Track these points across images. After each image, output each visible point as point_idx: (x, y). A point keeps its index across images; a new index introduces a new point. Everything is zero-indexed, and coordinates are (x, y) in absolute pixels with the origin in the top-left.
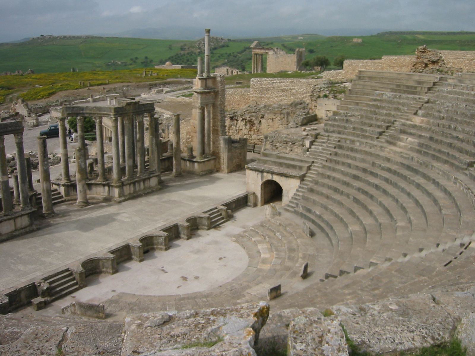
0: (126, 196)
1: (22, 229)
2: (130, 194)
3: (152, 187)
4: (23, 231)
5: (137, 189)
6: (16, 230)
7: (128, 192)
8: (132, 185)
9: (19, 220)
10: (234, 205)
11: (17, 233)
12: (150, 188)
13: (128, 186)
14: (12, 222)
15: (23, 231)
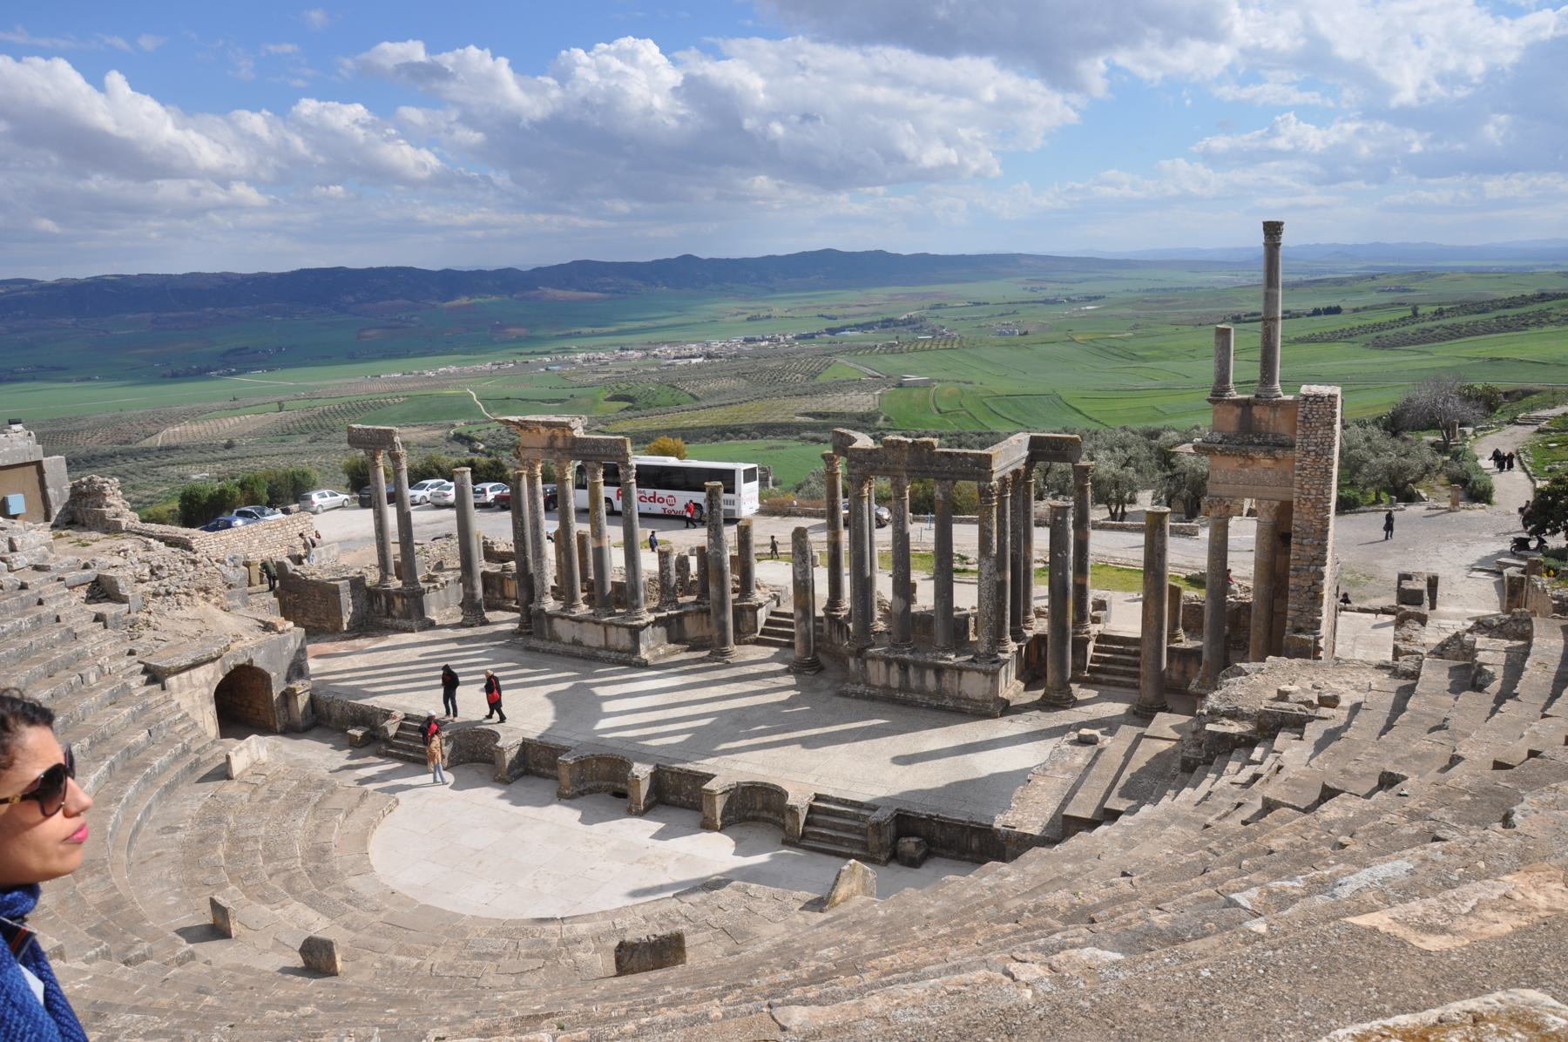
0: (875, 687)
1: (617, 651)
2: (887, 687)
3: (967, 699)
4: (613, 655)
5: (914, 683)
6: (607, 648)
7: (883, 681)
8: (895, 668)
9: (612, 631)
10: (975, 843)
11: (602, 654)
12: (957, 697)
13: (882, 665)
14: (600, 628)
15: (613, 655)
